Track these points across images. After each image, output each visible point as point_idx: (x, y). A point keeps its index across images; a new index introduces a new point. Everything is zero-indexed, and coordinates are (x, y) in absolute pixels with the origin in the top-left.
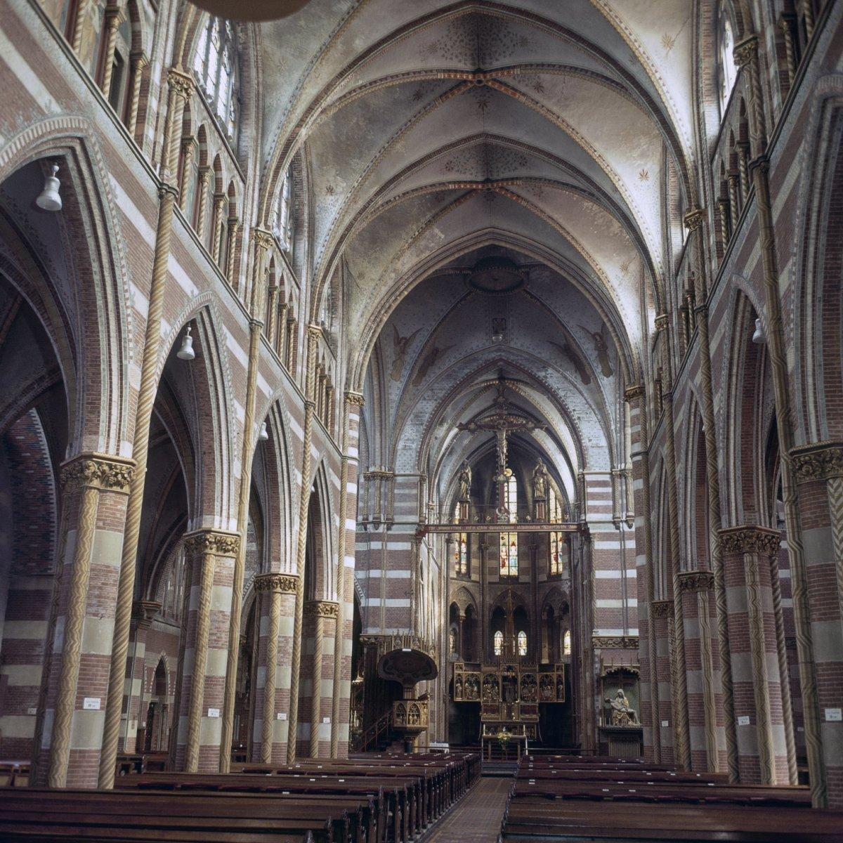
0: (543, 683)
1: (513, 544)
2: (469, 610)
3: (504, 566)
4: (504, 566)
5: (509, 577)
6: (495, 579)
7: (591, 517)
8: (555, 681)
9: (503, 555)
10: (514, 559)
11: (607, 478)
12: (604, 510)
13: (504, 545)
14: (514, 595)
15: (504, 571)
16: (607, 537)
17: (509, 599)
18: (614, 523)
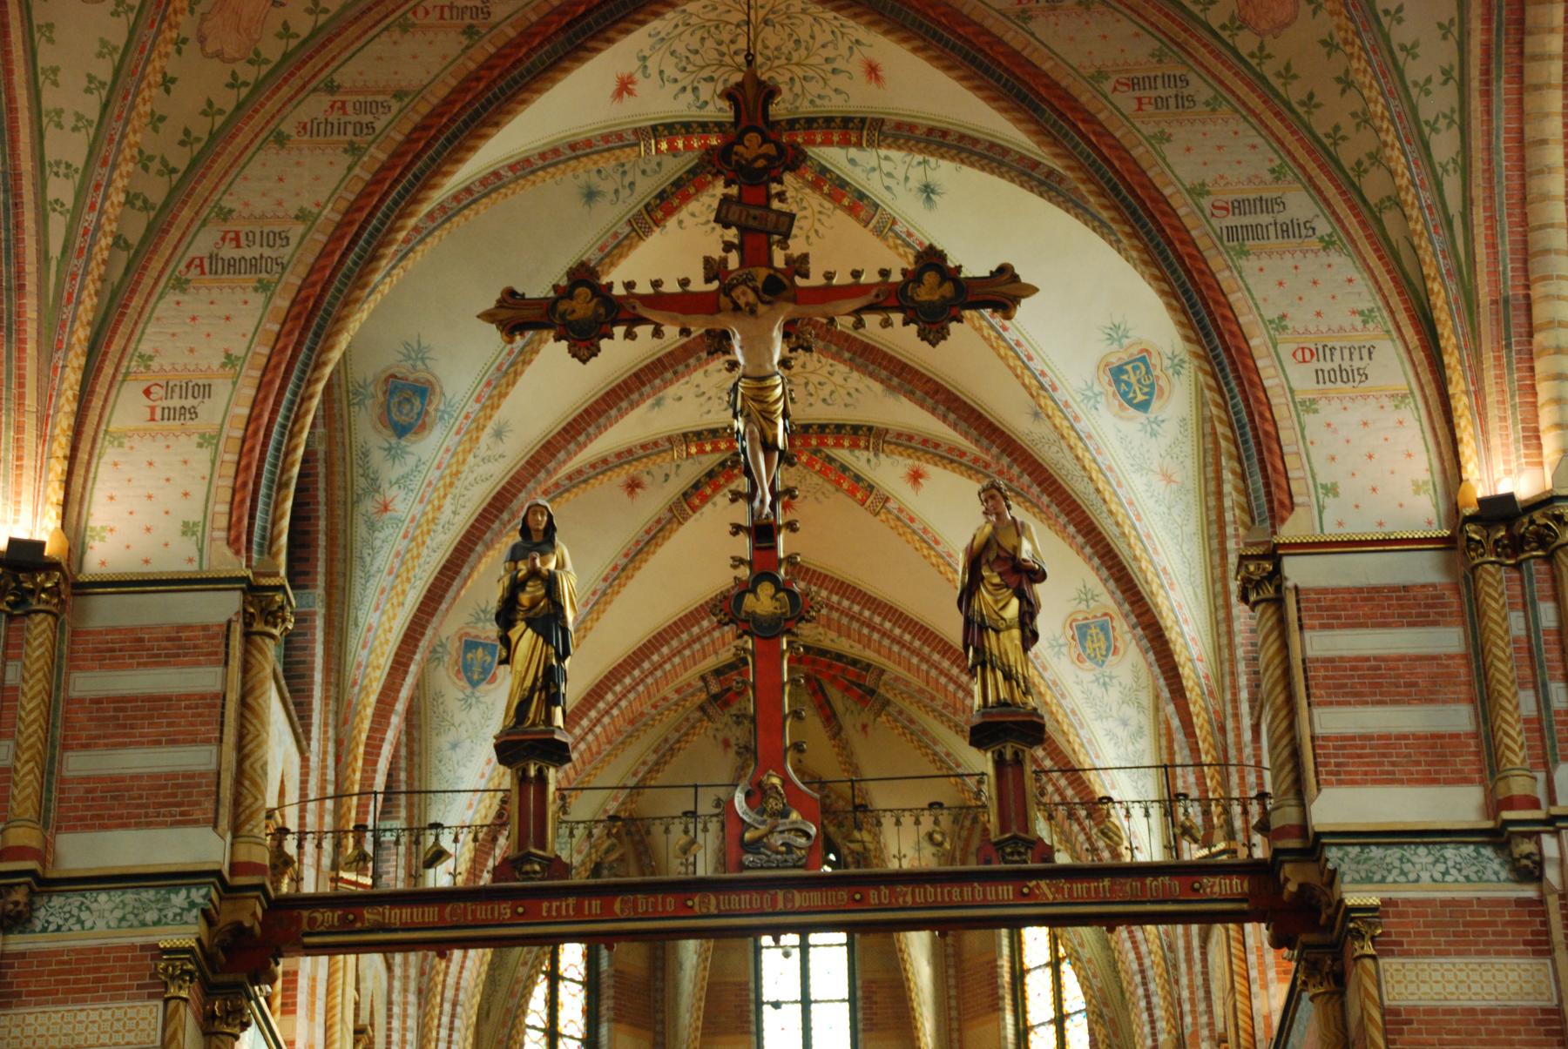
7: (1334, 808)
11: (1422, 570)
12: (1429, 761)
16: (1459, 929)
18: (1497, 837)
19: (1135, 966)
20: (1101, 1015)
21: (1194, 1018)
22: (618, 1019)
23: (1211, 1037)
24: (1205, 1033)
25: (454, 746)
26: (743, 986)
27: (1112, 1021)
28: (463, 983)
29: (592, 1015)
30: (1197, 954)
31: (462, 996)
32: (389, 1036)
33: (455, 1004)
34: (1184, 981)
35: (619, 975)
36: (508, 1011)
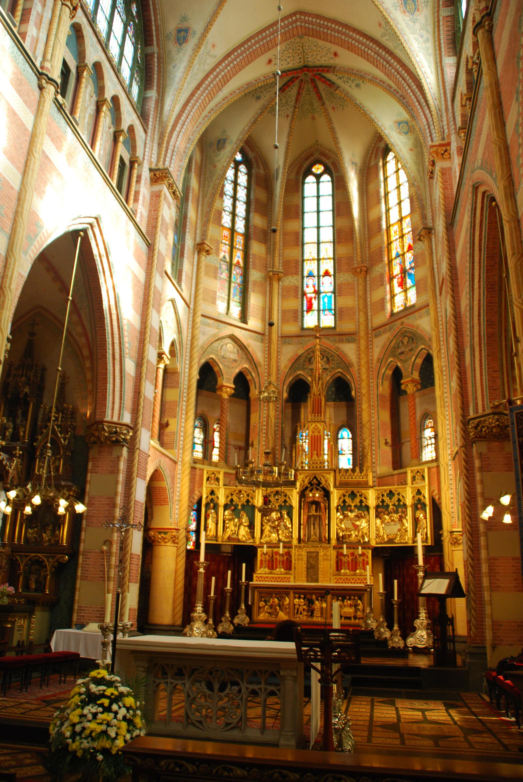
0: (381, 509)
1: (327, 274)
2: (242, 381)
3: (310, 308)
4: (310, 308)
5: (318, 328)
6: (292, 329)
8: (409, 501)
9: (309, 290)
10: (327, 300)
13: (310, 275)
14: (327, 357)
15: (310, 321)
17: (319, 364)
19: (425, 123)
20: (414, 184)
21: (449, 130)
22: (256, 211)
23: (456, 132)
24: (453, 131)
25: (174, 67)
26: (297, 206)
27: (417, 186)
28: (177, 145)
29: (248, 211)
30: (450, 107)
31: (176, 149)
32: (144, 153)
33: (173, 152)
34: (445, 119)
35: (257, 200)
36: (212, 194)
